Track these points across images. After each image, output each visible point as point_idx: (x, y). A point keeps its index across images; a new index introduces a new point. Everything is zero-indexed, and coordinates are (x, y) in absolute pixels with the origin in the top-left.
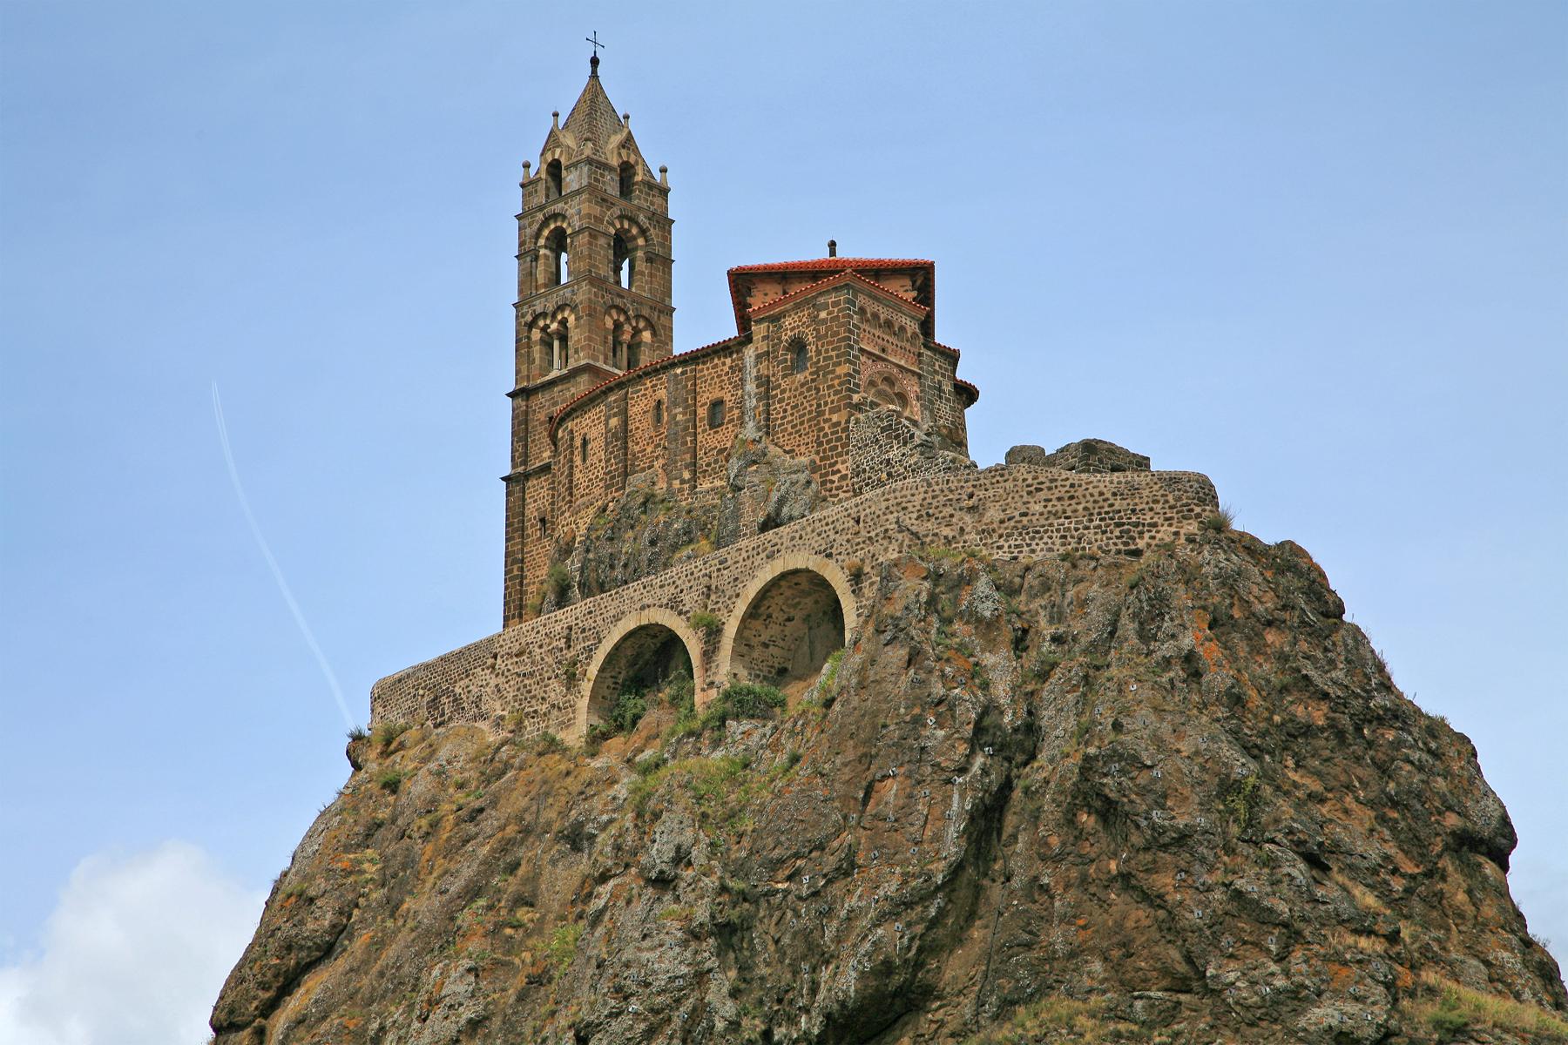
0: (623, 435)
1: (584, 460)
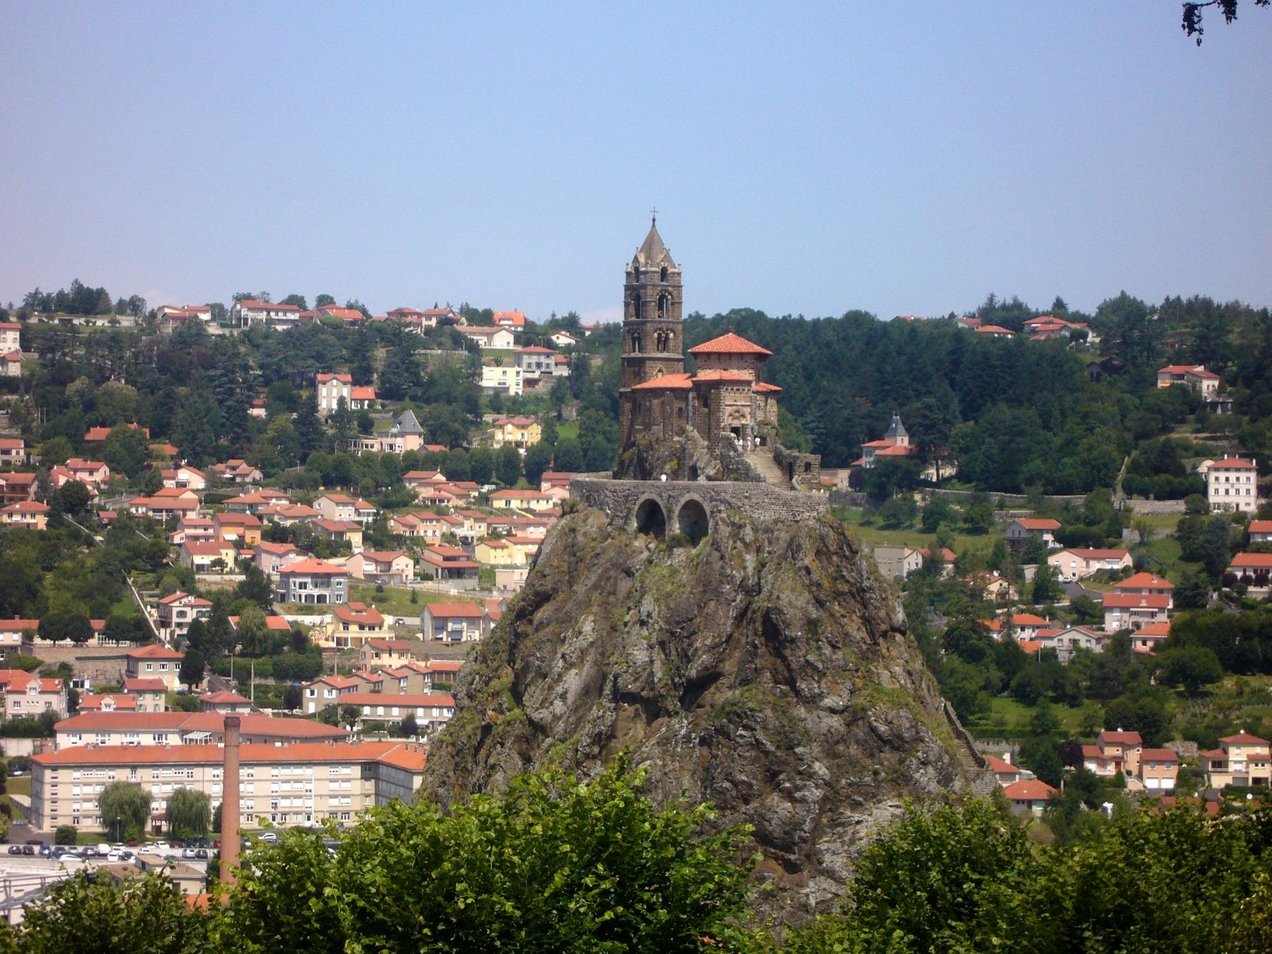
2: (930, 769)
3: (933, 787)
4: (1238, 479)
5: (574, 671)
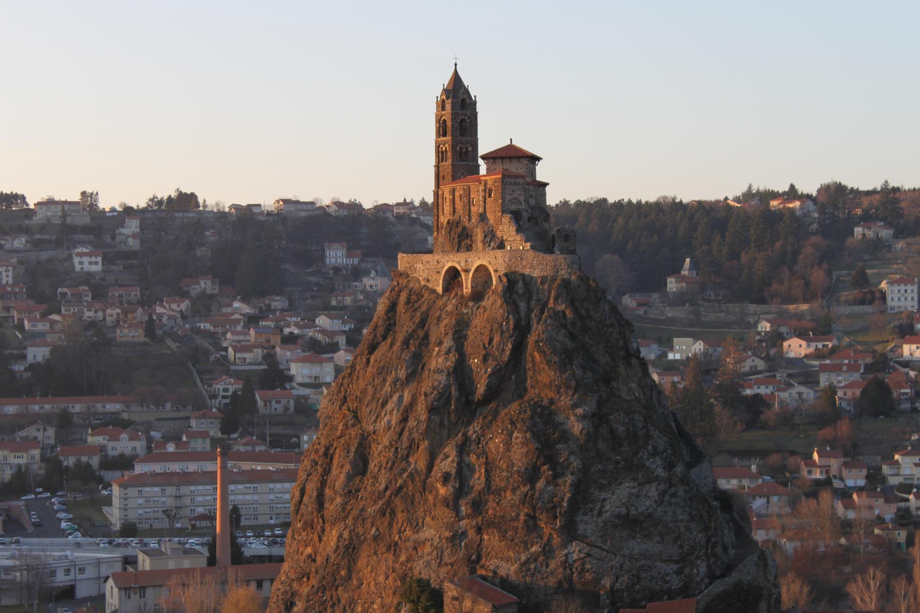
0: (453, 201)
2: (658, 459)
3: (660, 472)
4: (906, 291)
5: (397, 394)
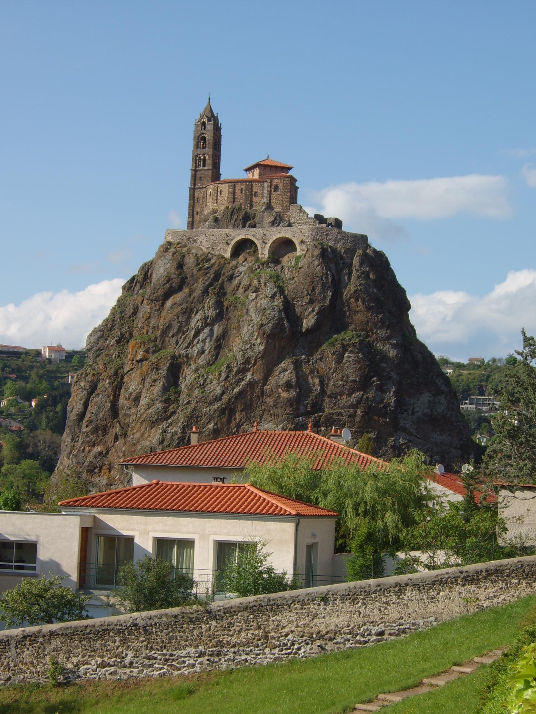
1: (221, 194)
